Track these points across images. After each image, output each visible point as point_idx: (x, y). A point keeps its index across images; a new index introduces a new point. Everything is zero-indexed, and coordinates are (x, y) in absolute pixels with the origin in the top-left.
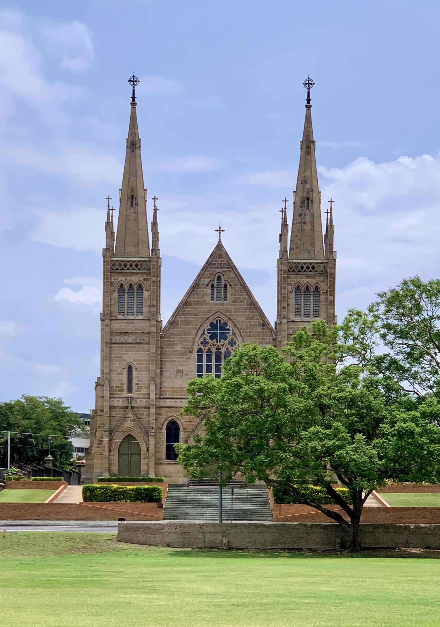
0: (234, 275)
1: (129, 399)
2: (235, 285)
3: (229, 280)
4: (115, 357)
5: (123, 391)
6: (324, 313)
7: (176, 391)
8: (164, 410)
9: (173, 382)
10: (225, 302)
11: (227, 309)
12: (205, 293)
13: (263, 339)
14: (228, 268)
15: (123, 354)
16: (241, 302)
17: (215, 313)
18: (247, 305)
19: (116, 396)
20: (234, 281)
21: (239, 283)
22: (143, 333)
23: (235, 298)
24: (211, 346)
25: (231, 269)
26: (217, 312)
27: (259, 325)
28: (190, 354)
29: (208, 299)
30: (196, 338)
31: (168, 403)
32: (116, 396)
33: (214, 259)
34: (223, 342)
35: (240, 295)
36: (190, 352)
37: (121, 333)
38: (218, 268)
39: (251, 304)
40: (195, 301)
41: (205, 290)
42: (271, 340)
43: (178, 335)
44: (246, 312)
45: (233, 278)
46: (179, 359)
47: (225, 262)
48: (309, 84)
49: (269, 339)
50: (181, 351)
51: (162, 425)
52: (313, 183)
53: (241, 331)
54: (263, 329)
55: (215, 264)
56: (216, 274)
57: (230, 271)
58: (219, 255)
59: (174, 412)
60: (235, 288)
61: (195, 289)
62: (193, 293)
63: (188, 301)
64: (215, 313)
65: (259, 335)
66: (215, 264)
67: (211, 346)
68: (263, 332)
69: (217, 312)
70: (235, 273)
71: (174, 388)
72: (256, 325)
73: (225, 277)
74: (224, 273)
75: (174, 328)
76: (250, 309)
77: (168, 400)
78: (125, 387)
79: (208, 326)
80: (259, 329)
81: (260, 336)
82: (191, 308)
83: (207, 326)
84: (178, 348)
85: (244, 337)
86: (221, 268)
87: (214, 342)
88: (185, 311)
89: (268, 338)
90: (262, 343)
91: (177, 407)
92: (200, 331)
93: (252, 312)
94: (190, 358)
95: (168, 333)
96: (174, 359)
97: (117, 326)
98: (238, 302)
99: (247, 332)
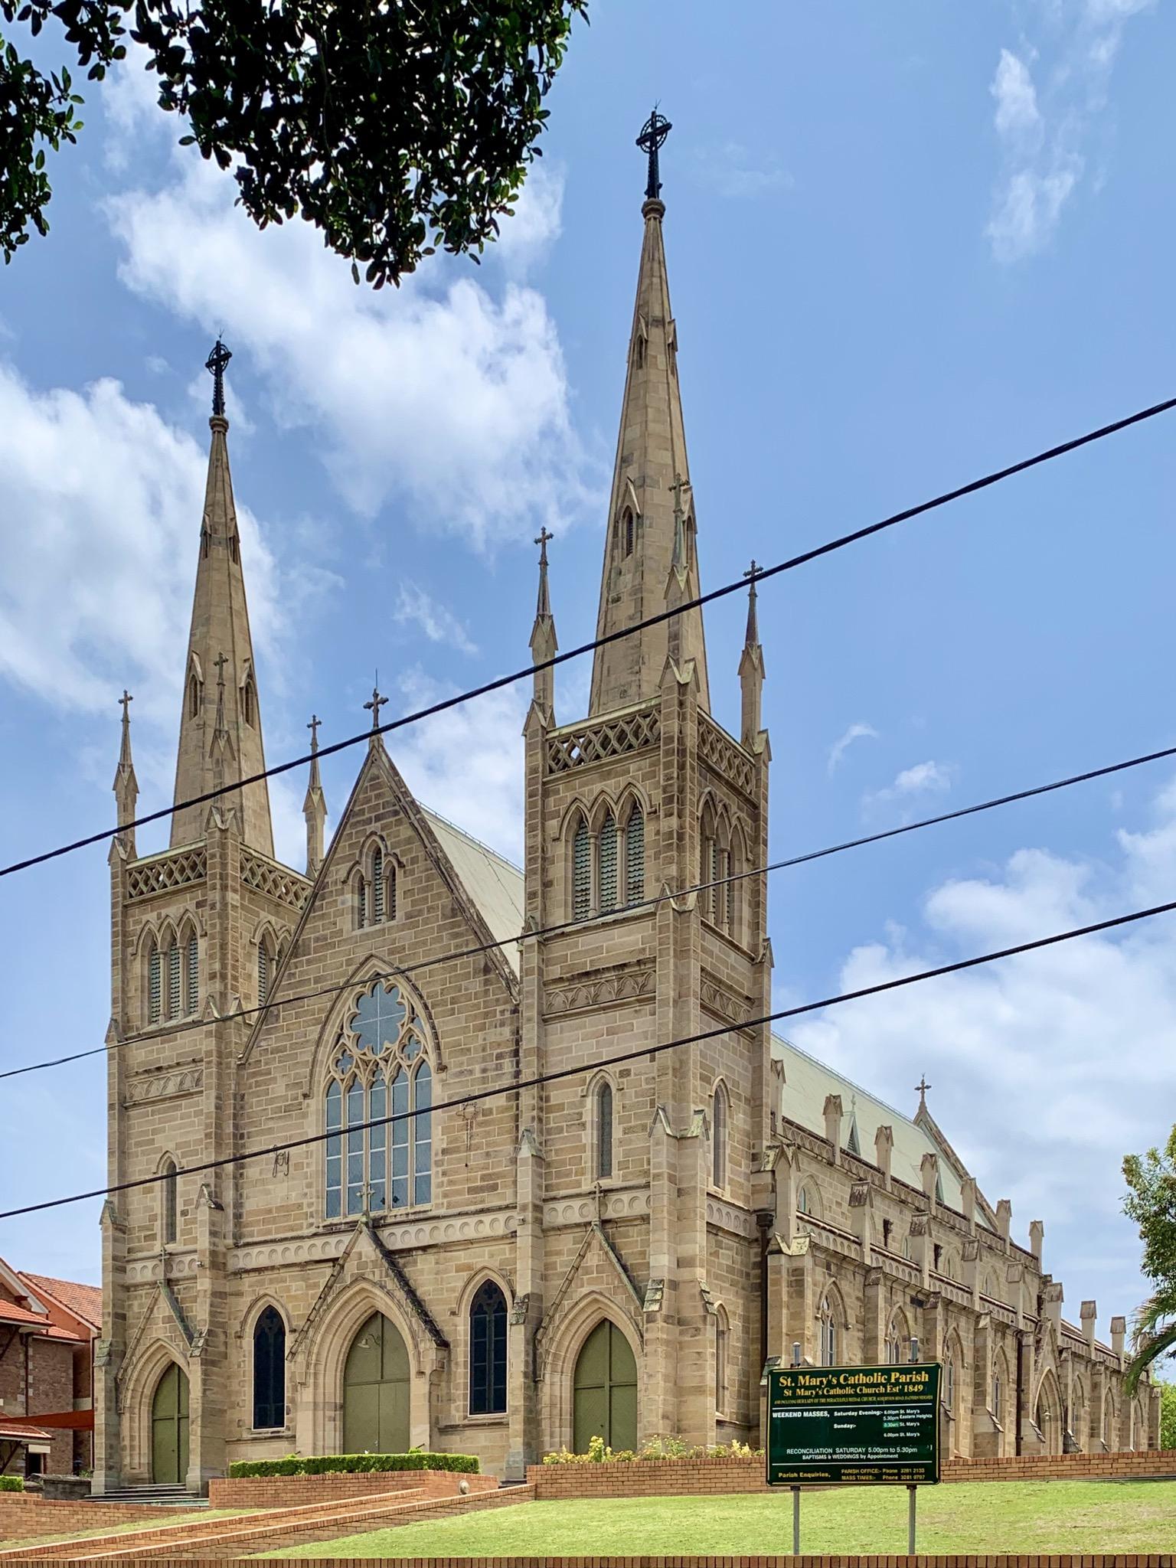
0: (410, 832)
1: (169, 1258)
2: (414, 860)
3: (397, 851)
4: (138, 1144)
5: (153, 1237)
6: (654, 884)
7: (274, 1220)
8: (248, 1280)
9: (268, 1192)
10: (392, 923)
11: (394, 942)
12: (340, 907)
13: (486, 1015)
14: (396, 813)
15: (155, 1132)
16: (429, 910)
17: (362, 964)
18: (444, 917)
19: (140, 1255)
20: (410, 850)
21: (422, 854)
22: (194, 1061)
23: (414, 903)
24: (358, 1067)
25: (402, 815)
26: (367, 959)
27: (476, 973)
28: (307, 1101)
29: (346, 923)
30: (321, 1049)
31: (257, 1257)
32: (140, 1255)
33: (361, 796)
34: (387, 1049)
35: (426, 889)
36: (305, 1096)
37: (146, 1071)
38: (369, 821)
39: (453, 909)
40: (317, 940)
41: (340, 899)
42: (508, 1015)
43: (277, 1050)
44: (440, 939)
45: (409, 841)
46: (281, 1124)
47: (390, 798)
48: (653, 135)
49: (502, 1012)
50: (285, 1098)
51: (243, 1323)
52: (650, 457)
53: (429, 1003)
54: (487, 982)
55: (362, 812)
56: (364, 842)
57: (399, 822)
58: (372, 779)
59: (271, 1281)
60: (412, 872)
61: (317, 903)
62: (312, 915)
63: (300, 942)
64: (362, 964)
65: (475, 1005)
66: (362, 812)
67: (358, 1067)
68: (486, 992)
69: (367, 959)
70: (412, 824)
71: (270, 1211)
72: (467, 976)
73: (388, 843)
74: (384, 834)
75: (269, 1032)
76: (453, 925)
77: (256, 1250)
78: (159, 1227)
79: (349, 1009)
80: (476, 985)
81: (477, 1006)
82: (309, 962)
83: (347, 1008)
84: (279, 1089)
85: (436, 1022)
86: (378, 818)
87: (364, 1054)
88: (294, 974)
89: (499, 1008)
90: (482, 1028)
91: (273, 1268)
92: (328, 1028)
93: (456, 935)
94: (305, 1116)
95: (256, 1052)
96: (271, 1124)
97: (141, 1054)
98: (420, 912)
99: (444, 1003)
